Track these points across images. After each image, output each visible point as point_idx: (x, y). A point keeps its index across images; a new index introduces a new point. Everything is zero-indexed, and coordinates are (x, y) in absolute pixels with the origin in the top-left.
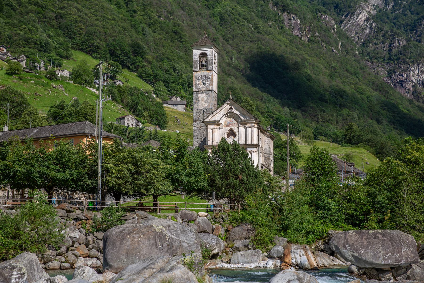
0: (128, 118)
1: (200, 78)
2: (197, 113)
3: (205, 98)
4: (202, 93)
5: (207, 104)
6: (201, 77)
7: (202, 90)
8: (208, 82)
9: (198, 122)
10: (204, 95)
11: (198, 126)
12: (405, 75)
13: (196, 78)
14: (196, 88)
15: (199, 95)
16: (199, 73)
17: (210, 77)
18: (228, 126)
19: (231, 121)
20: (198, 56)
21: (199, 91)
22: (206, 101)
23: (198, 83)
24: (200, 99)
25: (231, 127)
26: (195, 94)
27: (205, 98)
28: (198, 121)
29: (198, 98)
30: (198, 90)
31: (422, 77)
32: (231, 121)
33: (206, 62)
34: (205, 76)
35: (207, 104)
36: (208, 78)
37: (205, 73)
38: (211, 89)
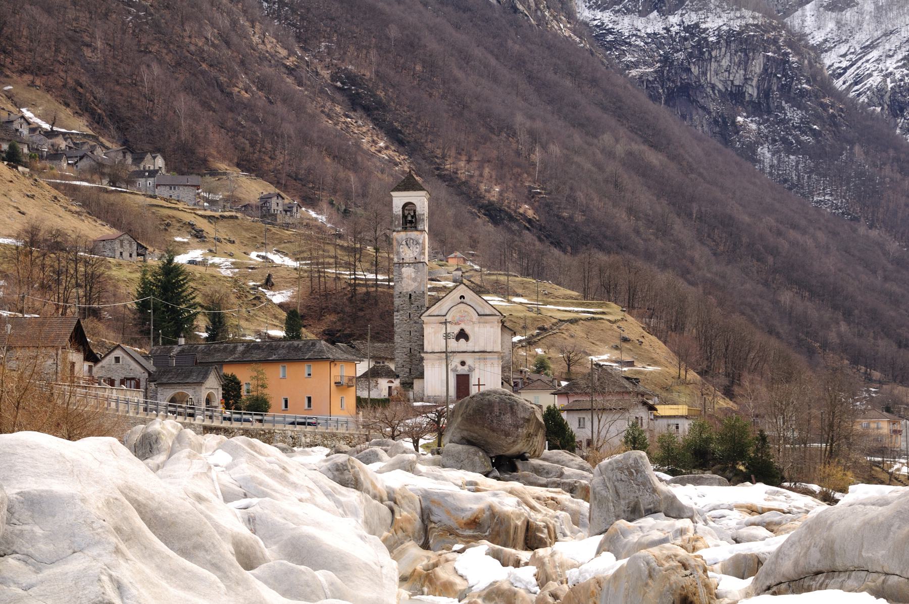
0: (122, 241)
1: (404, 243)
3: (413, 275)
5: (416, 284)
12: (695, 70)
13: (398, 242)
14: (398, 259)
15: (404, 270)
16: (403, 234)
17: (421, 241)
18: (457, 323)
22: (414, 280)
24: (404, 275)
25: (462, 326)
26: (396, 269)
27: (413, 275)
29: (400, 274)
31: (737, 75)
33: (412, 217)
35: (416, 284)
36: (418, 243)
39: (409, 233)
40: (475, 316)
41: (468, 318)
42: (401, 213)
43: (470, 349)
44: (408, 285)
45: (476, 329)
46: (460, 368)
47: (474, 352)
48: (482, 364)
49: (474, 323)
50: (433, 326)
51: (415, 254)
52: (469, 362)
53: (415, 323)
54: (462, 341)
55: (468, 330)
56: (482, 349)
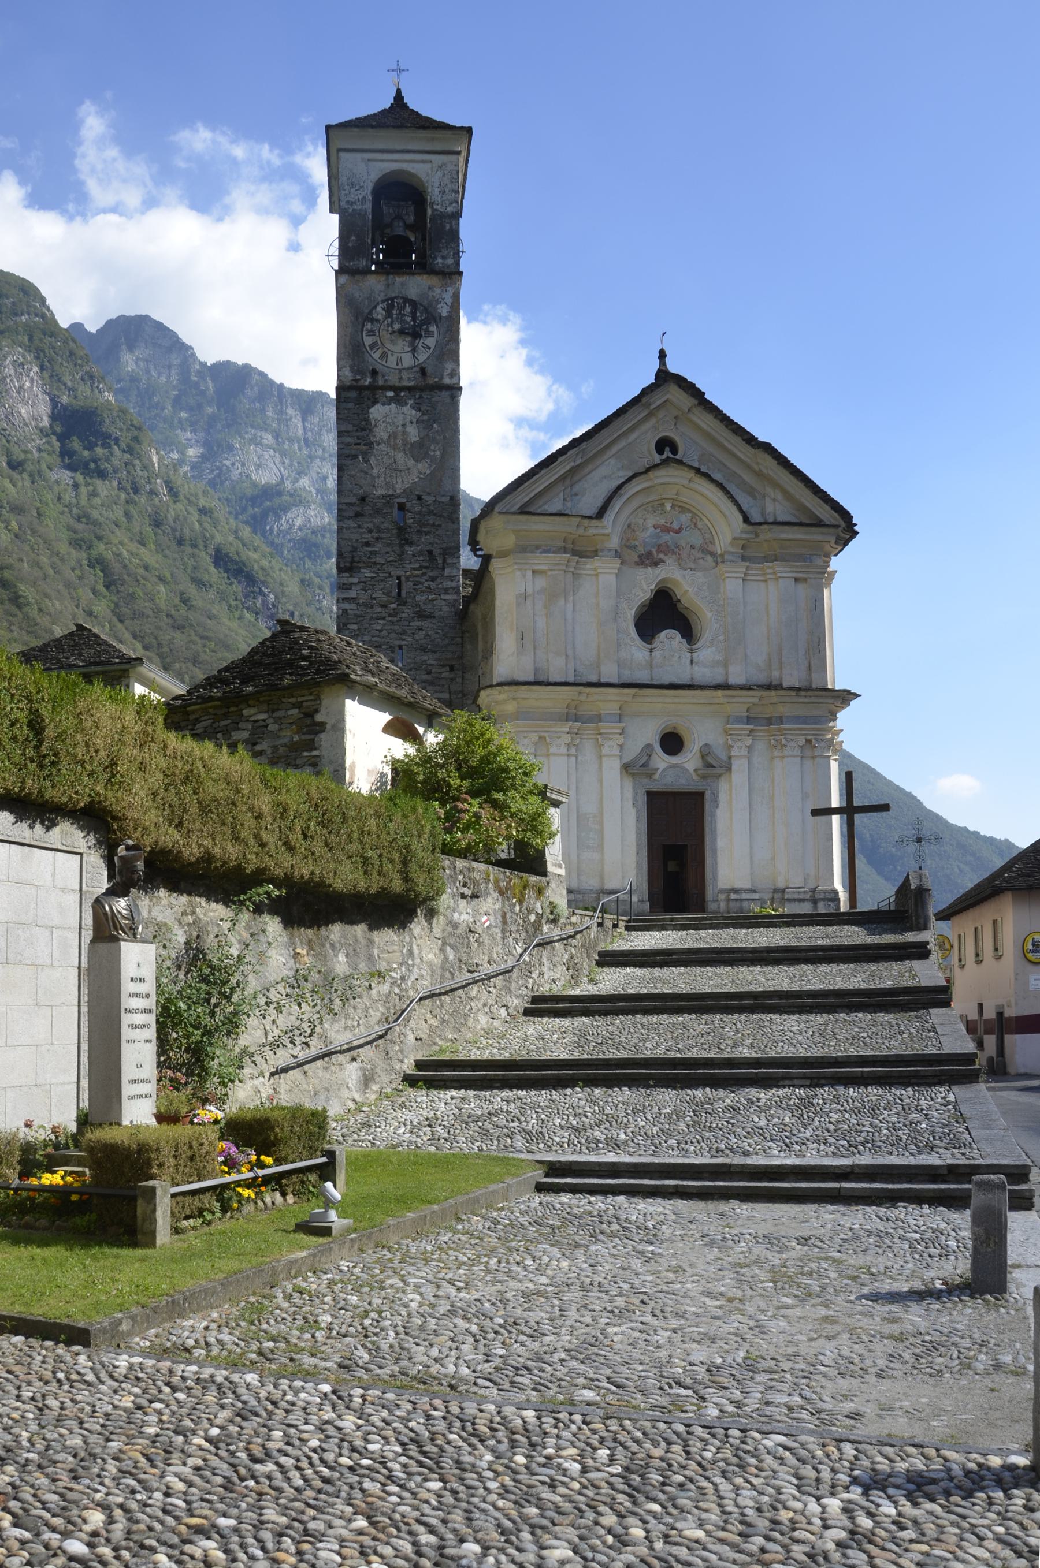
1: (380, 312)
2: (358, 515)
3: (413, 434)
4: (398, 401)
5: (424, 467)
6: (388, 310)
7: (393, 380)
8: (431, 342)
9: (368, 573)
10: (408, 411)
11: (364, 597)
15: (377, 412)
17: (444, 311)
19: (667, 530)
20: (367, 192)
21: (373, 388)
22: (418, 450)
23: (368, 341)
24: (380, 433)
25: (669, 571)
27: (413, 434)
28: (370, 565)
30: (368, 381)
32: (667, 530)
34: (414, 304)
35: (424, 467)
36: (432, 317)
37: (415, 286)
38: (447, 381)
39: (399, 280)
40: (725, 526)
41: (697, 540)
42: (368, 206)
43: (702, 674)
44: (394, 469)
45: (732, 585)
46: (661, 761)
47: (725, 686)
48: (760, 746)
49: (719, 559)
50: (542, 562)
51: (422, 357)
52: (703, 731)
53: (421, 615)
54: (669, 639)
55: (690, 587)
56: (762, 678)
